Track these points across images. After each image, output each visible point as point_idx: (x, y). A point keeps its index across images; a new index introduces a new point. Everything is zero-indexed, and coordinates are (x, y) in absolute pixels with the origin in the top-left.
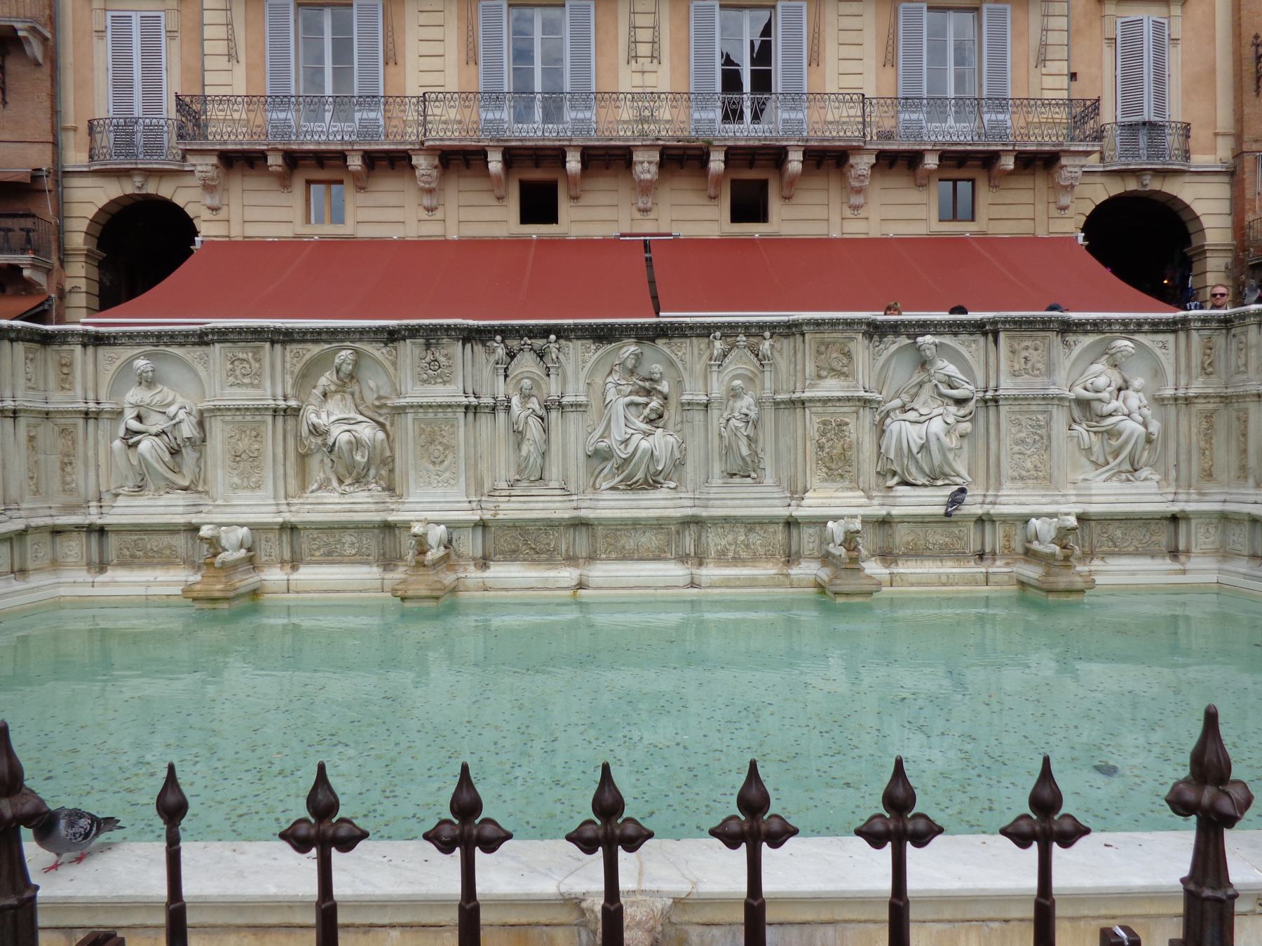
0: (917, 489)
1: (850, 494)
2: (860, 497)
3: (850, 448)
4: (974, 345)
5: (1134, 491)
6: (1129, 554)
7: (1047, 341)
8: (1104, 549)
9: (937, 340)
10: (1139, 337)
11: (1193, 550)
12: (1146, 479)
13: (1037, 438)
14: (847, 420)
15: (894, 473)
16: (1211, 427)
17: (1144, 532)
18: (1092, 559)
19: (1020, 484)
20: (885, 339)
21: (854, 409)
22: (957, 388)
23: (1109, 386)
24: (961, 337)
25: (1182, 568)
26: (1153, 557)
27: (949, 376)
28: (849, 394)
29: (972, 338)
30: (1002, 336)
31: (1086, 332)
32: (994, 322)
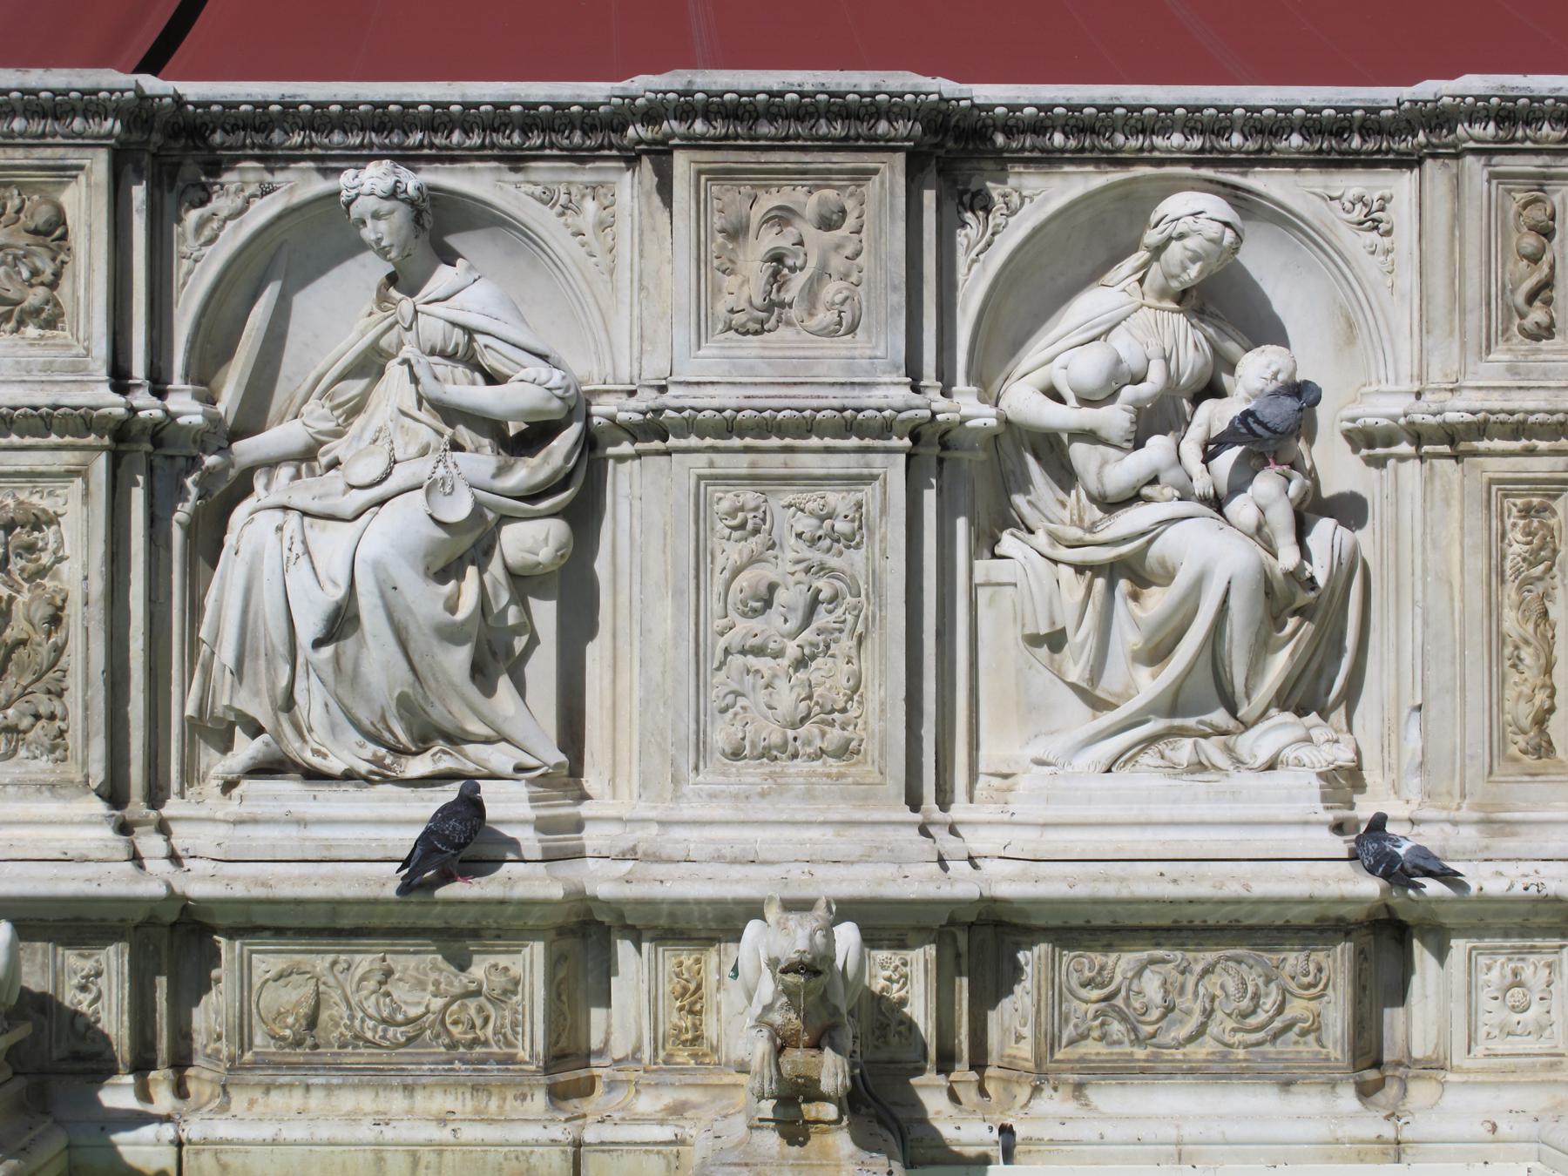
0: (323, 790)
1: (50, 808)
2: (88, 822)
3: (55, 620)
4: (590, 206)
5: (1224, 811)
6: (1191, 1071)
7: (872, 186)
8: (1092, 1048)
9: (412, 181)
10: (1265, 183)
11: (1458, 1057)
12: (1271, 766)
13: (825, 586)
14: (47, 504)
15: (255, 730)
16: (1543, 552)
17: (1254, 979)
18: (1037, 1090)
19: (751, 774)
20: (231, 178)
21: (68, 459)
22: (492, 378)
23: (1138, 379)
24: (542, 172)
25: (1388, 1131)
26: (1286, 1085)
27: (470, 331)
28: (42, 397)
29: (586, 175)
30: (682, 164)
31: (1049, 160)
32: (652, 115)
